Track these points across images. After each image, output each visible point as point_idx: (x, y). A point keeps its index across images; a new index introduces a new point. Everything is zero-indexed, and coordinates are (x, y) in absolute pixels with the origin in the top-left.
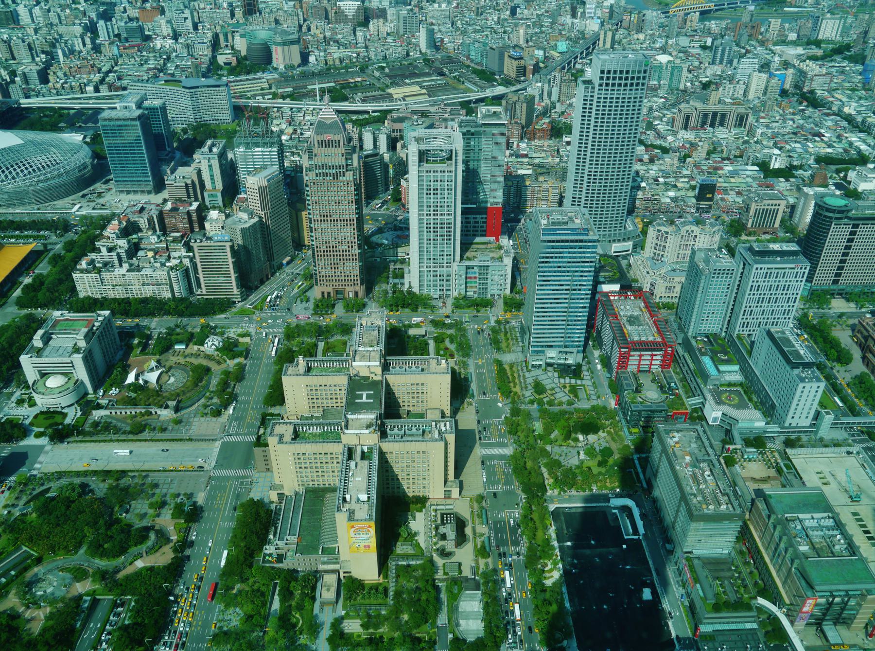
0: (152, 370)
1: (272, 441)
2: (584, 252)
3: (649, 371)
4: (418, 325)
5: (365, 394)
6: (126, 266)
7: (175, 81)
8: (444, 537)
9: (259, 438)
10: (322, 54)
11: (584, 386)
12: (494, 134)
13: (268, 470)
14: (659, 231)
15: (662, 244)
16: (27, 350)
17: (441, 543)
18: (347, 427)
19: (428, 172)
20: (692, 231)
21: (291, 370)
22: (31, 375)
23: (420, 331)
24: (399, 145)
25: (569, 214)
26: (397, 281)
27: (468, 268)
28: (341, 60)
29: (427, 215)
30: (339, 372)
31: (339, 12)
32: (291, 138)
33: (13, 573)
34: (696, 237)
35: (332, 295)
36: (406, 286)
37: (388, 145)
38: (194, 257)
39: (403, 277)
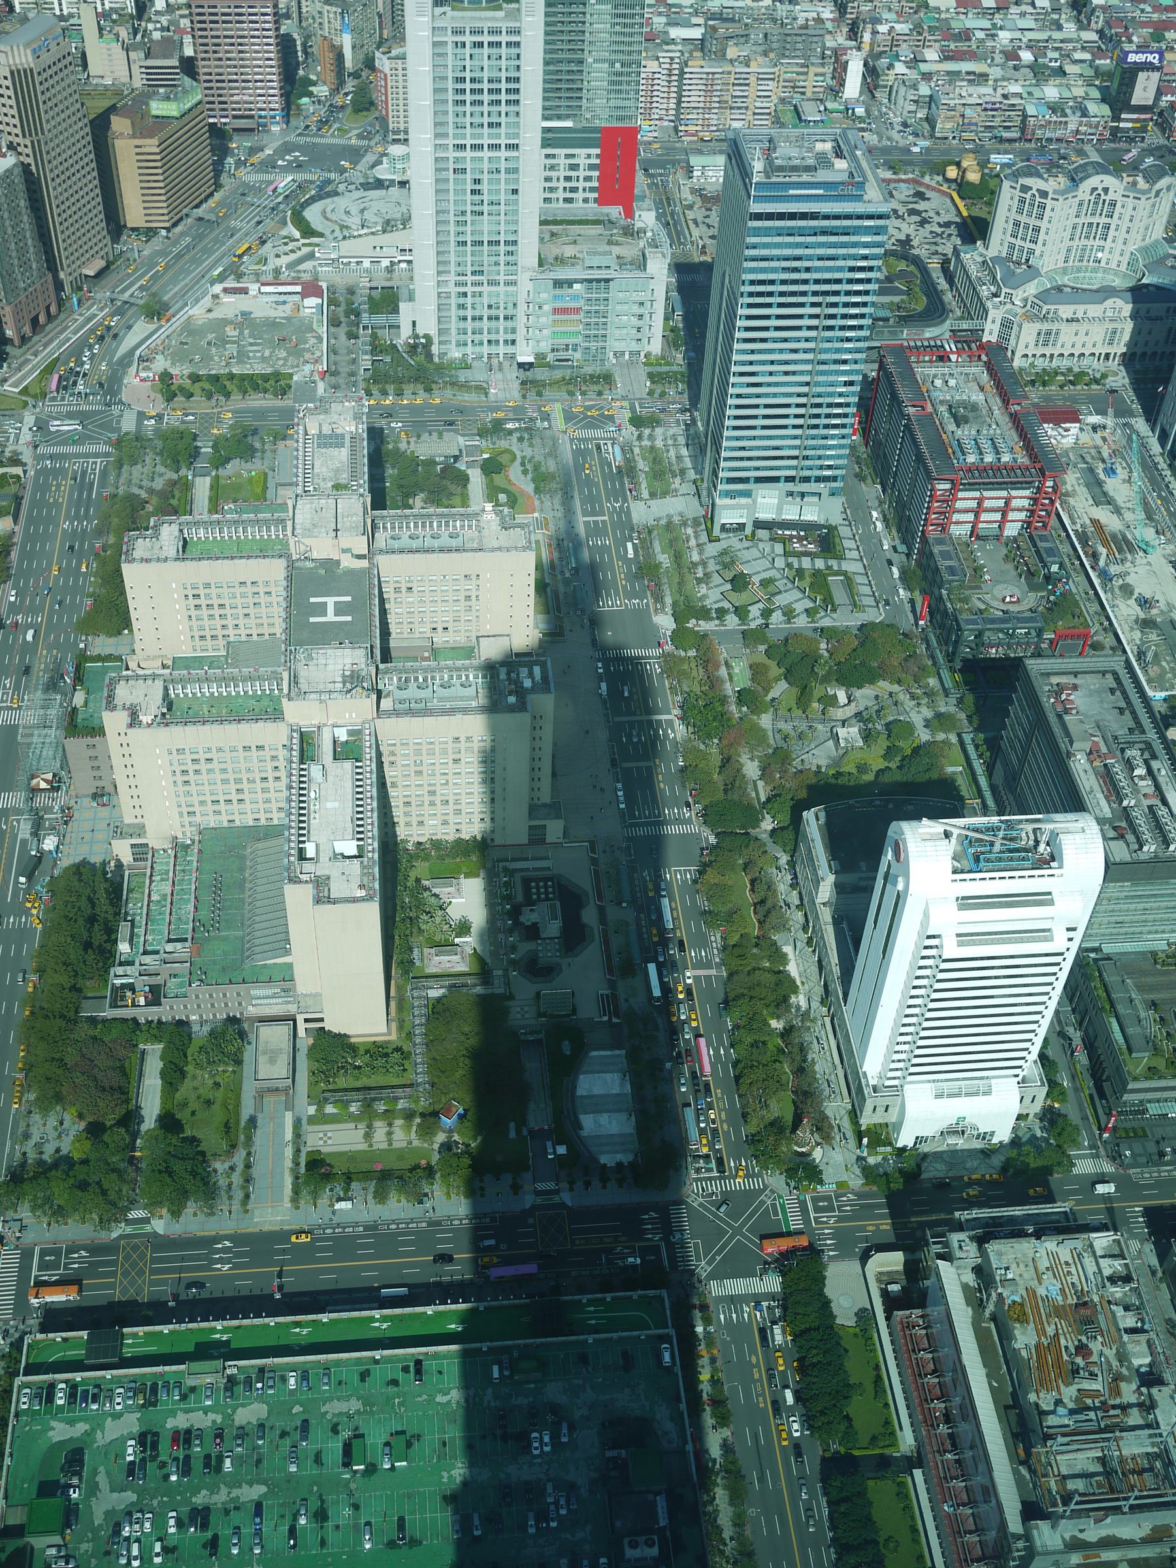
1: (114, 722)
2: (855, 245)
3: (998, 538)
5: (331, 601)
8: (532, 932)
11: (845, 574)
14: (1025, 189)
15: (1032, 222)
17: (530, 946)
20: (1106, 190)
21: (141, 547)
25: (819, 146)
26: (380, 319)
27: (558, 284)
30: (263, 551)
34: (1113, 204)
36: (406, 332)
39: (396, 311)
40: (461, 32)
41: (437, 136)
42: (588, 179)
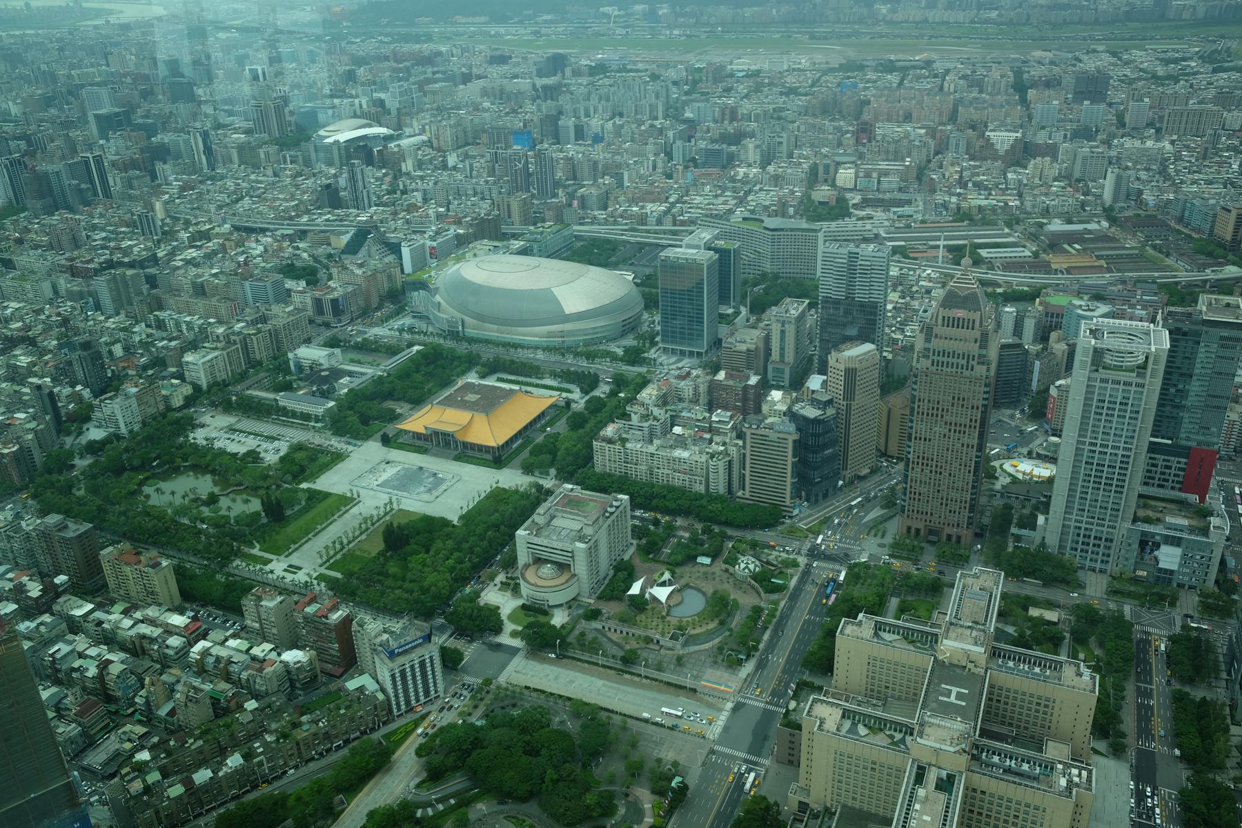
0: (663, 584)
4: (1050, 605)
5: (955, 690)
6: (657, 442)
7: (756, 220)
9: (788, 711)
10: (954, 199)
12: (1222, 338)
13: (791, 763)
16: (526, 525)
18: (921, 734)
19: (1102, 381)
21: (849, 629)
22: (523, 557)
23: (1051, 616)
24: (1054, 336)
28: (980, 208)
29: (1091, 444)
31: (989, 144)
32: (894, 308)
33: (452, 801)
35: (922, 532)
37: (1035, 334)
38: (744, 447)
40: (1106, 381)
41: (1080, 436)
42: (1178, 476)
